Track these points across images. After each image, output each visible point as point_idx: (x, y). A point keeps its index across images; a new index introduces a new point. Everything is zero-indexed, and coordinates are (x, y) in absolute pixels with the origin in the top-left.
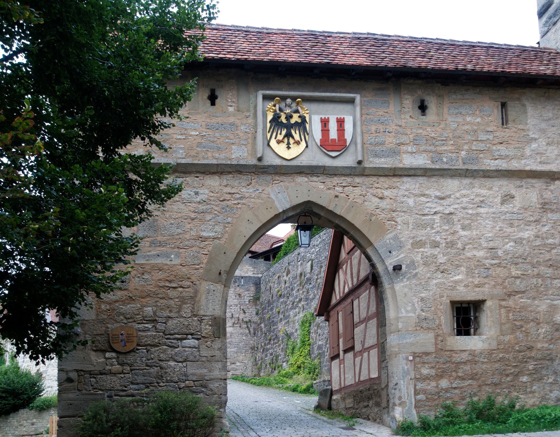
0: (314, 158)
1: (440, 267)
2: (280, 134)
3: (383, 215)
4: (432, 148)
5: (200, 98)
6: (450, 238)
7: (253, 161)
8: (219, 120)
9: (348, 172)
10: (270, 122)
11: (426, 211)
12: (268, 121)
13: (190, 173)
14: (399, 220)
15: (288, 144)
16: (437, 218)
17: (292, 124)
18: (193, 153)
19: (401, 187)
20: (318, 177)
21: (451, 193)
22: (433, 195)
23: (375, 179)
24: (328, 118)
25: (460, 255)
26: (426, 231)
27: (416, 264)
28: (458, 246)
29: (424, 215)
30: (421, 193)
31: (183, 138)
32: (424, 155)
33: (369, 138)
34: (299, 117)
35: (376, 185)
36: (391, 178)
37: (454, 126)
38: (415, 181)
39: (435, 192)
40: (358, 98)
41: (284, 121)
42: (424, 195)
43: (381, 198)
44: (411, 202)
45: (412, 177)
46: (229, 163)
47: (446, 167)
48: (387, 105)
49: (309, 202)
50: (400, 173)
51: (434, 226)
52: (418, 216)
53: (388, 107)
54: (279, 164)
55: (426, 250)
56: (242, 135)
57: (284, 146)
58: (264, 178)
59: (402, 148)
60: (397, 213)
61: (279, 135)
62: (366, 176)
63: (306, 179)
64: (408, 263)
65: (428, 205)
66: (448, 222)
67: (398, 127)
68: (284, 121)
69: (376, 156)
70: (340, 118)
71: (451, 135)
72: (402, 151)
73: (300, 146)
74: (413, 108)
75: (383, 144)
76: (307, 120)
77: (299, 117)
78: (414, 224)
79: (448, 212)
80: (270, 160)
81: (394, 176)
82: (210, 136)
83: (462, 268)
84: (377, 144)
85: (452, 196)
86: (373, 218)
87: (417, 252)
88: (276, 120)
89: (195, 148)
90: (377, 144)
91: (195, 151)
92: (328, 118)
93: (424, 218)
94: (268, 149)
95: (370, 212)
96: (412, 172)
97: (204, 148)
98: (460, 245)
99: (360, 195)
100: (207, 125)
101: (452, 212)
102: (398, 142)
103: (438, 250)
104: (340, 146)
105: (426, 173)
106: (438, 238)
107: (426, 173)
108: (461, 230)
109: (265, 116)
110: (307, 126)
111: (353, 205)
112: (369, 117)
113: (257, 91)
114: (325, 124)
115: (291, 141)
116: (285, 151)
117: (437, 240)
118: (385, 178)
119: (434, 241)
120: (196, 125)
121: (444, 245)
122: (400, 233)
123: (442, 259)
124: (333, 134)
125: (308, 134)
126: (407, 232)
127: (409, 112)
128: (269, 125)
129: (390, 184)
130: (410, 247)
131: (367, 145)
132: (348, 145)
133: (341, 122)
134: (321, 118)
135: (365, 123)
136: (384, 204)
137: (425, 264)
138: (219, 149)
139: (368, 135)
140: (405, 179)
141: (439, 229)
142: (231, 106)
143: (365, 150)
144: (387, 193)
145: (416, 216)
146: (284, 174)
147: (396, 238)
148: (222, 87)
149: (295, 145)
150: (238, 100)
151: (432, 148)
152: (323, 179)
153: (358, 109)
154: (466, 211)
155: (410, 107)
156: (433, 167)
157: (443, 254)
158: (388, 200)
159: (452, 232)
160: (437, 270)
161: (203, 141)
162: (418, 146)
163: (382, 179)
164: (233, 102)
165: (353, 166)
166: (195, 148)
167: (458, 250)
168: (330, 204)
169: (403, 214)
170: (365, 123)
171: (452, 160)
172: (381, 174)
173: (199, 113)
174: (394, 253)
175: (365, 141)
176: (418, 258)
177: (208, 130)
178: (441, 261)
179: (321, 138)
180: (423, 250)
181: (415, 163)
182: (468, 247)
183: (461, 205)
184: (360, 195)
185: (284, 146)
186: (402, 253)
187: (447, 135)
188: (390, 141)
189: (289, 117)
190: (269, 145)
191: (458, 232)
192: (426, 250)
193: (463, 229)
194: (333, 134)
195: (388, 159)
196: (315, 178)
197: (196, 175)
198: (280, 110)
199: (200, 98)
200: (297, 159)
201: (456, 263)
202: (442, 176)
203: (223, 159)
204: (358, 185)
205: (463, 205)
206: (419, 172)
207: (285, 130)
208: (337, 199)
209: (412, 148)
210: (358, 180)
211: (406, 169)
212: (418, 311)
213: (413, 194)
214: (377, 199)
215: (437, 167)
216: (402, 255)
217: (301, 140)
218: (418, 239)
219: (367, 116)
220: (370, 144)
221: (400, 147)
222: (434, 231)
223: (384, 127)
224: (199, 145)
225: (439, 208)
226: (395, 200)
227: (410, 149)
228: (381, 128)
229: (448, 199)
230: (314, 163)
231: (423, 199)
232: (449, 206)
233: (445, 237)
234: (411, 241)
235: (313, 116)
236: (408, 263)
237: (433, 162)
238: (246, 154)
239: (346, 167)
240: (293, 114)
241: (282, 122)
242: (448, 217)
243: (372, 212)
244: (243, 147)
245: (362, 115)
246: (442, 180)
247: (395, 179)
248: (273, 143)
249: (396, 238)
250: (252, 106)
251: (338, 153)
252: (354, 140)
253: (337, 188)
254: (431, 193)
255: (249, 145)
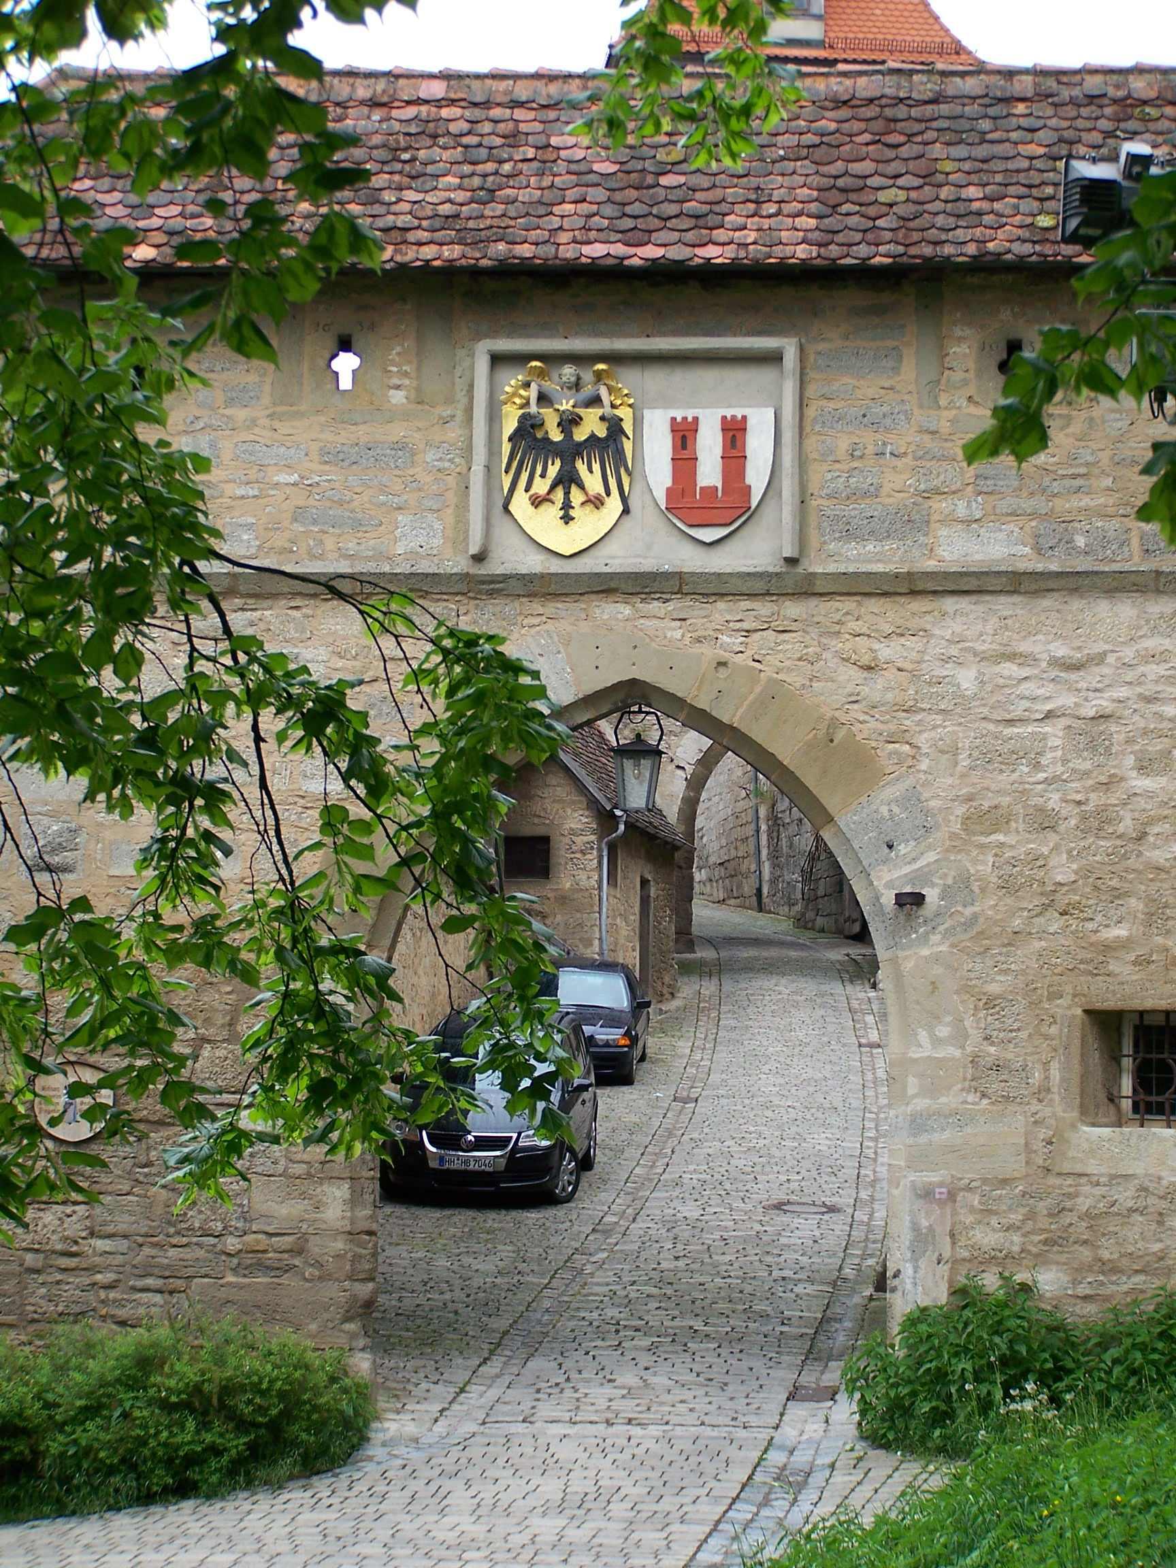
0: (649, 547)
1: (1058, 896)
2: (543, 476)
3: (873, 724)
4: (1039, 504)
5: (306, 366)
6: (1095, 799)
7: (457, 564)
8: (362, 433)
9: (759, 586)
10: (510, 439)
11: (1018, 711)
12: (505, 437)
13: (274, 596)
14: (922, 740)
15: (567, 506)
16: (1054, 732)
17: (580, 444)
18: (280, 541)
19: (937, 632)
20: (667, 601)
21: (1107, 647)
22: (1045, 656)
23: (849, 604)
24: (696, 419)
25: (1125, 857)
26: (1015, 776)
27: (975, 887)
28: (1121, 829)
29: (1010, 722)
30: (1002, 649)
31: (251, 493)
32: (1011, 526)
33: (829, 476)
34: (602, 418)
35: (853, 626)
36: (903, 600)
37: (1119, 424)
38: (981, 608)
39: (1051, 647)
40: (789, 347)
41: (556, 436)
42: (1012, 657)
43: (869, 668)
44: (967, 679)
45: (974, 598)
46: (387, 569)
47: (1083, 564)
48: (891, 364)
49: (633, 682)
50: (931, 586)
51: (1044, 761)
52: (991, 727)
53: (896, 370)
54: (538, 569)
55: (1011, 839)
56: (429, 479)
57: (552, 512)
58: (499, 608)
59: (935, 506)
60: (919, 717)
61: (537, 479)
62: (821, 595)
63: (626, 610)
64: (950, 881)
65: (1025, 688)
66: (1092, 746)
67: (927, 437)
68: (556, 436)
69: (849, 534)
70: (733, 417)
71: (1105, 457)
72: (935, 517)
73: (604, 510)
74: (979, 373)
75: (873, 493)
76: (628, 427)
77: (602, 418)
78: (976, 754)
79: (1092, 713)
80: (514, 559)
81: (913, 593)
82: (332, 485)
83: (1133, 902)
84: (853, 496)
85: (1111, 659)
86: (840, 735)
87: (982, 846)
88: (528, 430)
89: (286, 524)
90: (853, 496)
91: (287, 534)
92: (696, 419)
93: (1009, 731)
94: (506, 518)
95: (829, 715)
96: (973, 584)
97: (315, 522)
98: (1127, 825)
99: (800, 659)
100: (323, 452)
101: (1108, 711)
102: (922, 487)
103: (1053, 838)
104: (730, 508)
105: (1017, 583)
106: (1054, 800)
107: (1017, 583)
108: (1134, 774)
109: (494, 417)
110: (628, 446)
111: (774, 694)
112: (832, 405)
113: (478, 337)
114: (684, 438)
115: (577, 497)
116: (548, 531)
117: (1051, 805)
118: (883, 600)
119: (1041, 810)
120: (293, 451)
121: (1073, 822)
122: (926, 784)
123: (1063, 871)
124: (709, 473)
125: (629, 474)
126: (950, 781)
127: (965, 382)
128: (506, 448)
129: (900, 622)
130: (956, 827)
131: (820, 501)
132: (754, 504)
133: (734, 432)
134: (673, 419)
135: (817, 428)
136: (876, 688)
137: (1008, 887)
138: (357, 525)
139: (825, 467)
140: (950, 604)
141: (1059, 769)
142: (398, 387)
143: (813, 520)
144: (885, 651)
145: (984, 724)
146: (555, 596)
147: (911, 799)
148: (372, 327)
149: (589, 507)
150: (418, 369)
151: (1039, 504)
152: (681, 609)
153: (789, 388)
154: (1155, 708)
155: (971, 365)
156: (1040, 567)
157: (1069, 852)
158: (892, 674)
159: (1103, 779)
160: (1045, 907)
161: (311, 502)
162: (992, 498)
163: (874, 605)
164: (406, 374)
165: (771, 569)
166: (286, 524)
167: (1119, 842)
168: (699, 689)
169: (938, 719)
170: (817, 428)
171: (1105, 542)
172: (868, 590)
173: (300, 415)
174: (902, 849)
175: (813, 487)
176: (985, 867)
177: (327, 468)
178: (1059, 878)
179: (669, 482)
180: (1000, 837)
181: (978, 557)
182: (1156, 830)
183: (1139, 690)
184: (800, 659)
185: (552, 512)
186: (930, 848)
187: (1090, 459)
188: (897, 483)
189: (569, 422)
190: (506, 508)
191: (1122, 779)
192: (1011, 839)
193: (1143, 768)
194: (709, 473)
195: (888, 546)
196: (655, 607)
197: (293, 604)
198: (543, 399)
199: (306, 366)
200: (592, 552)
201: (1115, 883)
202: (1075, 590)
203: (369, 559)
204: (794, 626)
205: (1148, 689)
206: (996, 584)
207: (558, 463)
208: (723, 673)
209: (969, 506)
210: (793, 609)
211: (947, 575)
212: (975, 1035)
213: (975, 655)
214: (854, 672)
215: (1054, 567)
216: (931, 857)
217: (608, 494)
218: (986, 805)
219: (824, 403)
220: (829, 497)
221: (930, 503)
222: (1041, 776)
223: (878, 436)
224: (298, 515)
225: (1066, 700)
226: (915, 676)
227: (961, 510)
228: (869, 440)
229: (1096, 670)
230: (648, 564)
231: (1010, 669)
232: (1096, 690)
233: (1078, 797)
234: (960, 810)
235: (647, 413)
236: (950, 881)
237: (1038, 550)
238: (437, 542)
239: (749, 574)
240: (581, 411)
241: (546, 440)
242: (1093, 732)
243: (837, 714)
244: (430, 517)
245: (802, 404)
246: (1076, 604)
247: (918, 605)
248: (520, 504)
249: (911, 799)
250: (460, 384)
251: (724, 532)
252: (775, 484)
253: (725, 639)
254: (1037, 649)
255: (450, 511)
